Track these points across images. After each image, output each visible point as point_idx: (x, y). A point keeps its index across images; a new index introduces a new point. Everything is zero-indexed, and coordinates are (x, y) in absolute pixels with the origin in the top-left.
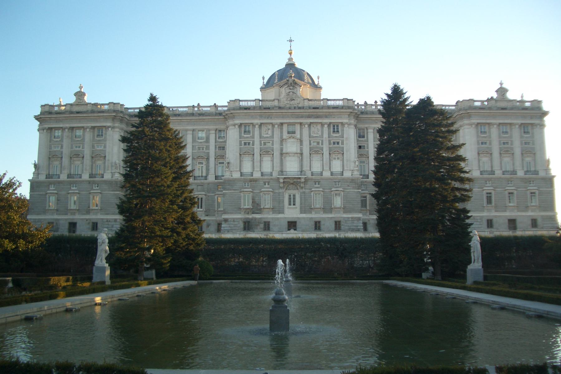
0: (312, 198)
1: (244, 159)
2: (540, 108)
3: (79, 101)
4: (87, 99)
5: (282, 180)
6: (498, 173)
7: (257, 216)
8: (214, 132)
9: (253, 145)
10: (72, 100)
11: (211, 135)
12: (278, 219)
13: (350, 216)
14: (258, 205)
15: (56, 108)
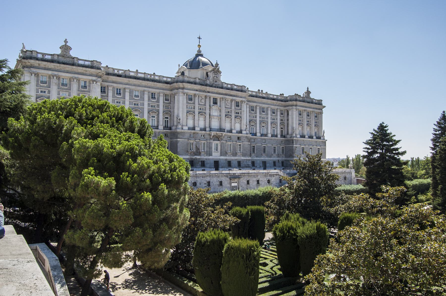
0: (227, 147)
1: (188, 118)
2: (321, 104)
3: (65, 53)
4: (73, 53)
5: (213, 135)
6: (307, 137)
7: (198, 157)
8: (162, 95)
9: (194, 109)
10: (59, 52)
11: (160, 97)
12: (209, 159)
13: (245, 158)
14: (199, 149)
15: (40, 56)
